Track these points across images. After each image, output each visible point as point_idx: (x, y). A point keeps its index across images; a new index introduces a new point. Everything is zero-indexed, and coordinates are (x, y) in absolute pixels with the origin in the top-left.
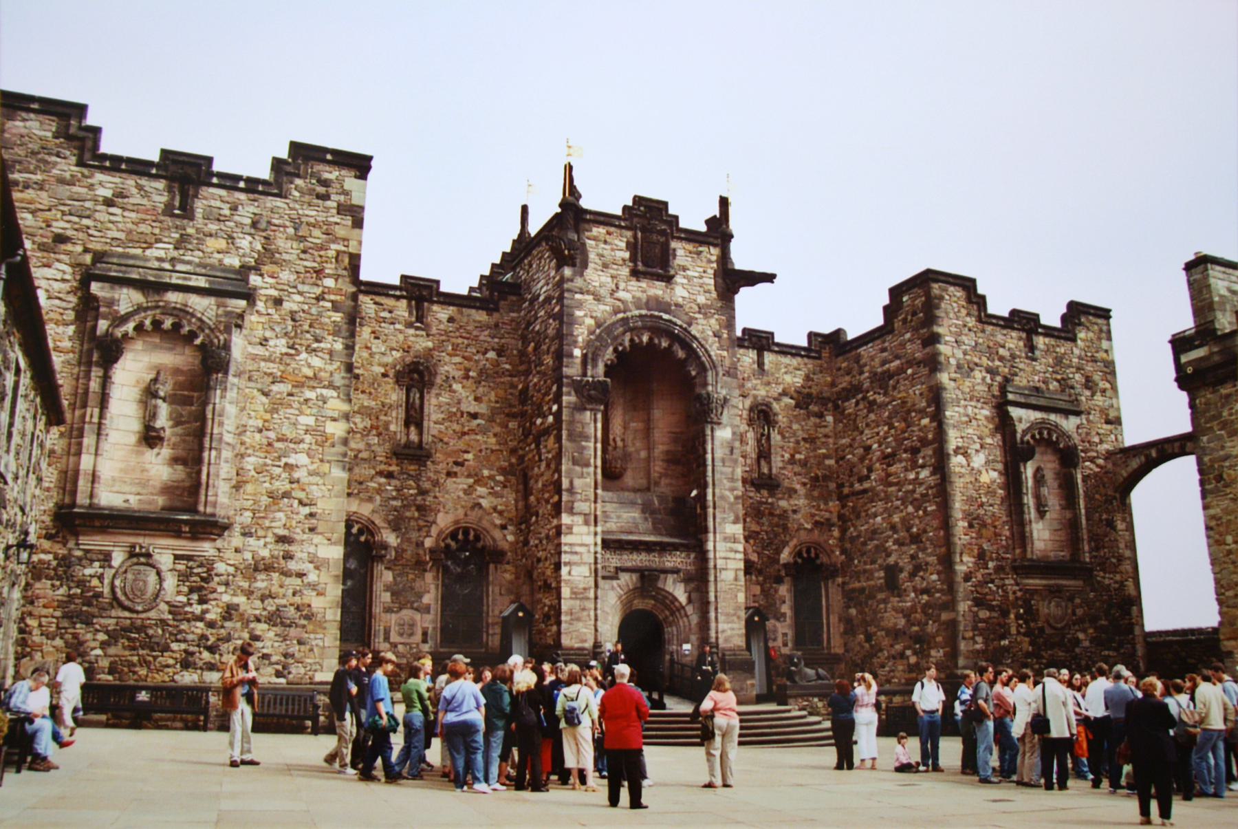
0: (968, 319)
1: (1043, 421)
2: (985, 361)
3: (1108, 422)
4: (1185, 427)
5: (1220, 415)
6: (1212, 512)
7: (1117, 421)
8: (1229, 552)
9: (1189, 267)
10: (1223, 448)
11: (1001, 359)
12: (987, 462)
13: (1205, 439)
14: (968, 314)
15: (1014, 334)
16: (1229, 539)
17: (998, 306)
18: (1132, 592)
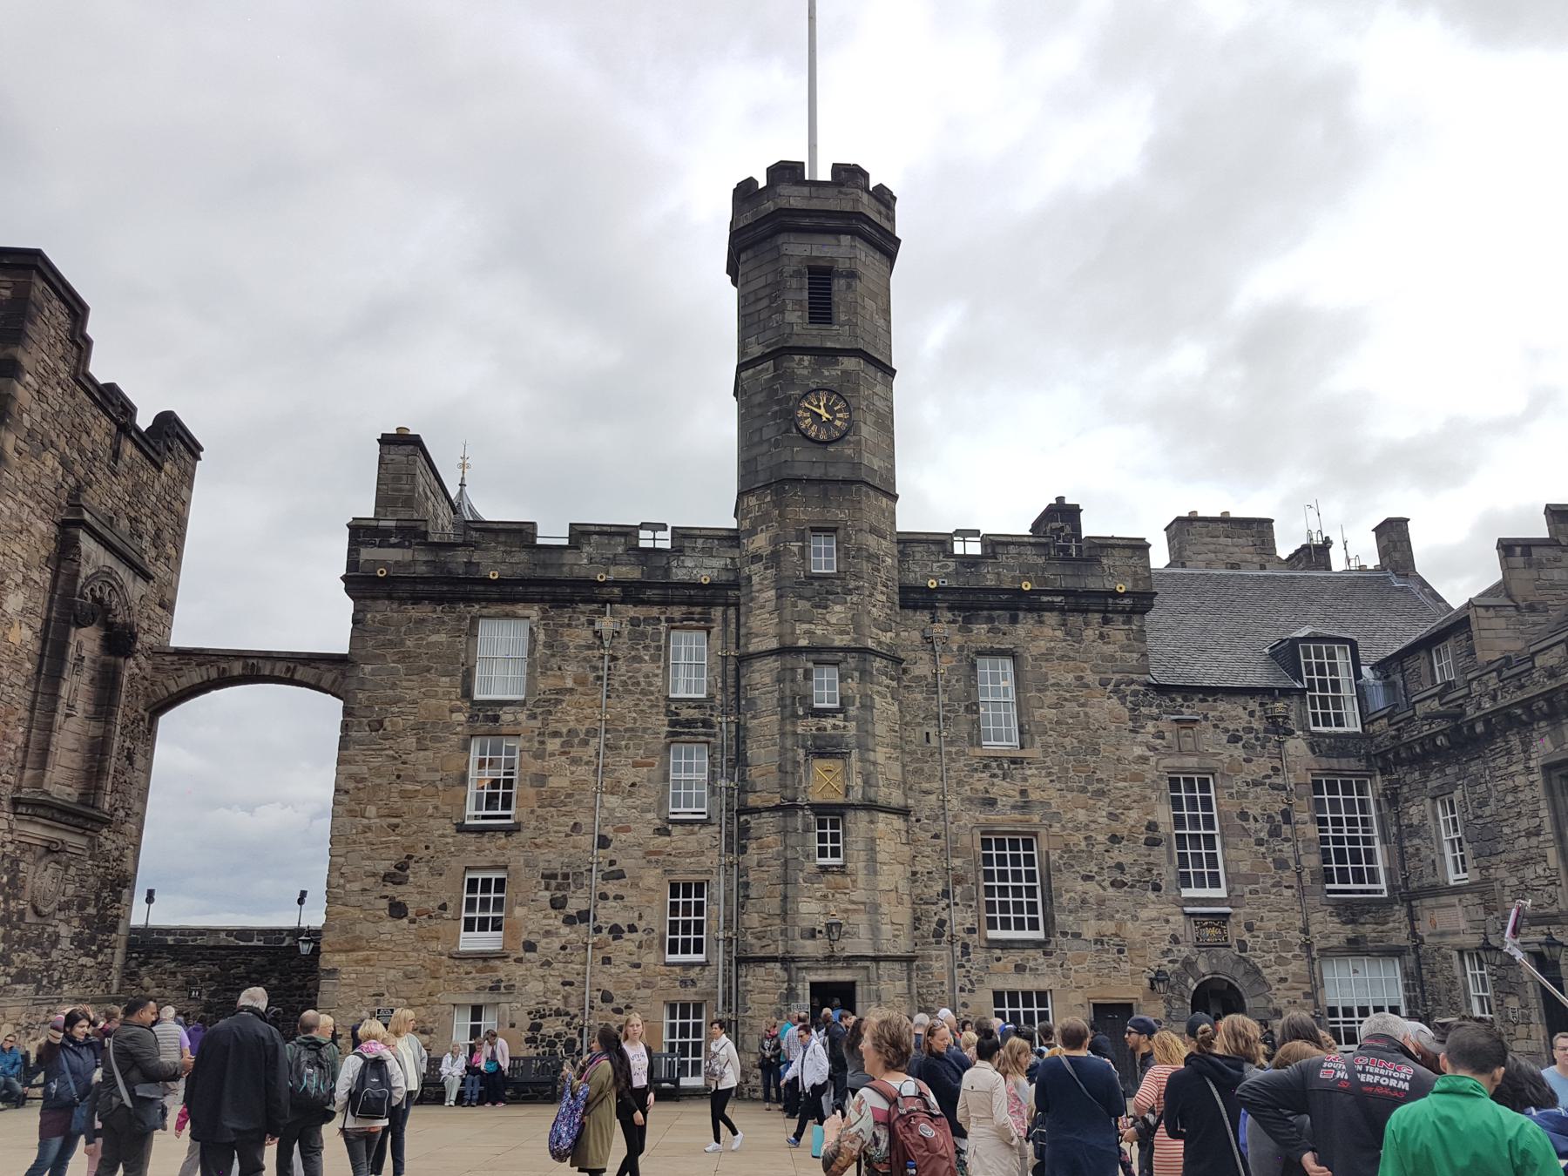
0: (61, 365)
1: (110, 573)
2: (62, 443)
3: (162, 605)
4: (341, 646)
5: (402, 643)
6: (354, 769)
7: (168, 606)
8: (368, 828)
9: (385, 440)
10: (394, 686)
11: (81, 451)
12: (25, 611)
13: (368, 668)
14: (63, 358)
15: (105, 421)
16: (371, 810)
17: (101, 369)
18: (130, 868)
